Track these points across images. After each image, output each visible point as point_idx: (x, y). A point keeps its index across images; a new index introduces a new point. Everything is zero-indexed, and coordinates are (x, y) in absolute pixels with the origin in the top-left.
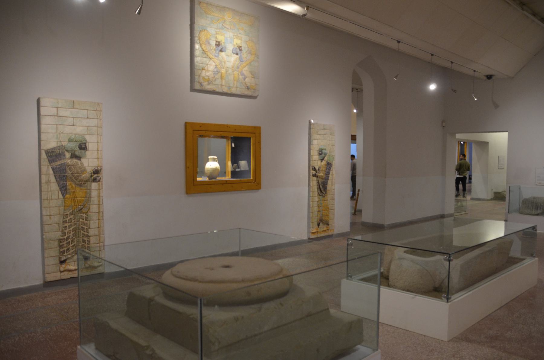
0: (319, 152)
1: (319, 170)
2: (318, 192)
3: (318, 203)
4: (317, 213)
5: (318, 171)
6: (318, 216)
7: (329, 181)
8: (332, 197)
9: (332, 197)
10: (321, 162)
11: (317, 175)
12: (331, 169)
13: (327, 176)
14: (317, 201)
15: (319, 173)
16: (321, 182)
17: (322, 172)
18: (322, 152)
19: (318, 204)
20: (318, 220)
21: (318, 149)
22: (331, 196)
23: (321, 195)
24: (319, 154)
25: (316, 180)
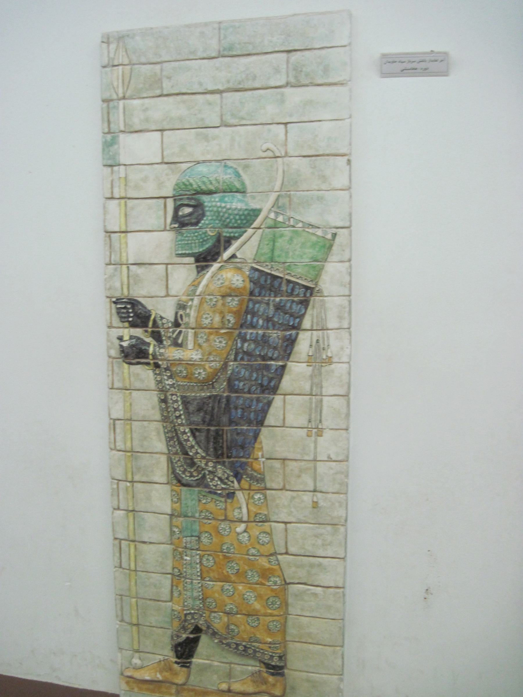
0: (177, 209)
1: (177, 324)
2: (170, 461)
3: (171, 526)
4: (167, 582)
5: (167, 333)
6: (171, 600)
7: (278, 401)
8: (315, 505)
9: (315, 505)
10: (198, 272)
11: (154, 357)
12: (307, 323)
13: (251, 368)
14: (169, 511)
15: (176, 344)
16: (186, 402)
17: (196, 335)
18: (198, 206)
19: (172, 533)
20: (176, 624)
21: (168, 191)
22: (307, 498)
23: (186, 478)
24: (176, 218)
25: (152, 384)
